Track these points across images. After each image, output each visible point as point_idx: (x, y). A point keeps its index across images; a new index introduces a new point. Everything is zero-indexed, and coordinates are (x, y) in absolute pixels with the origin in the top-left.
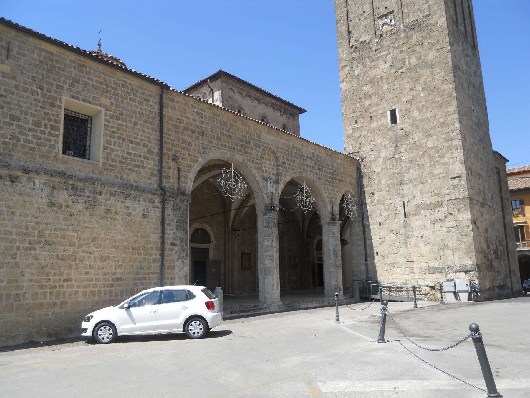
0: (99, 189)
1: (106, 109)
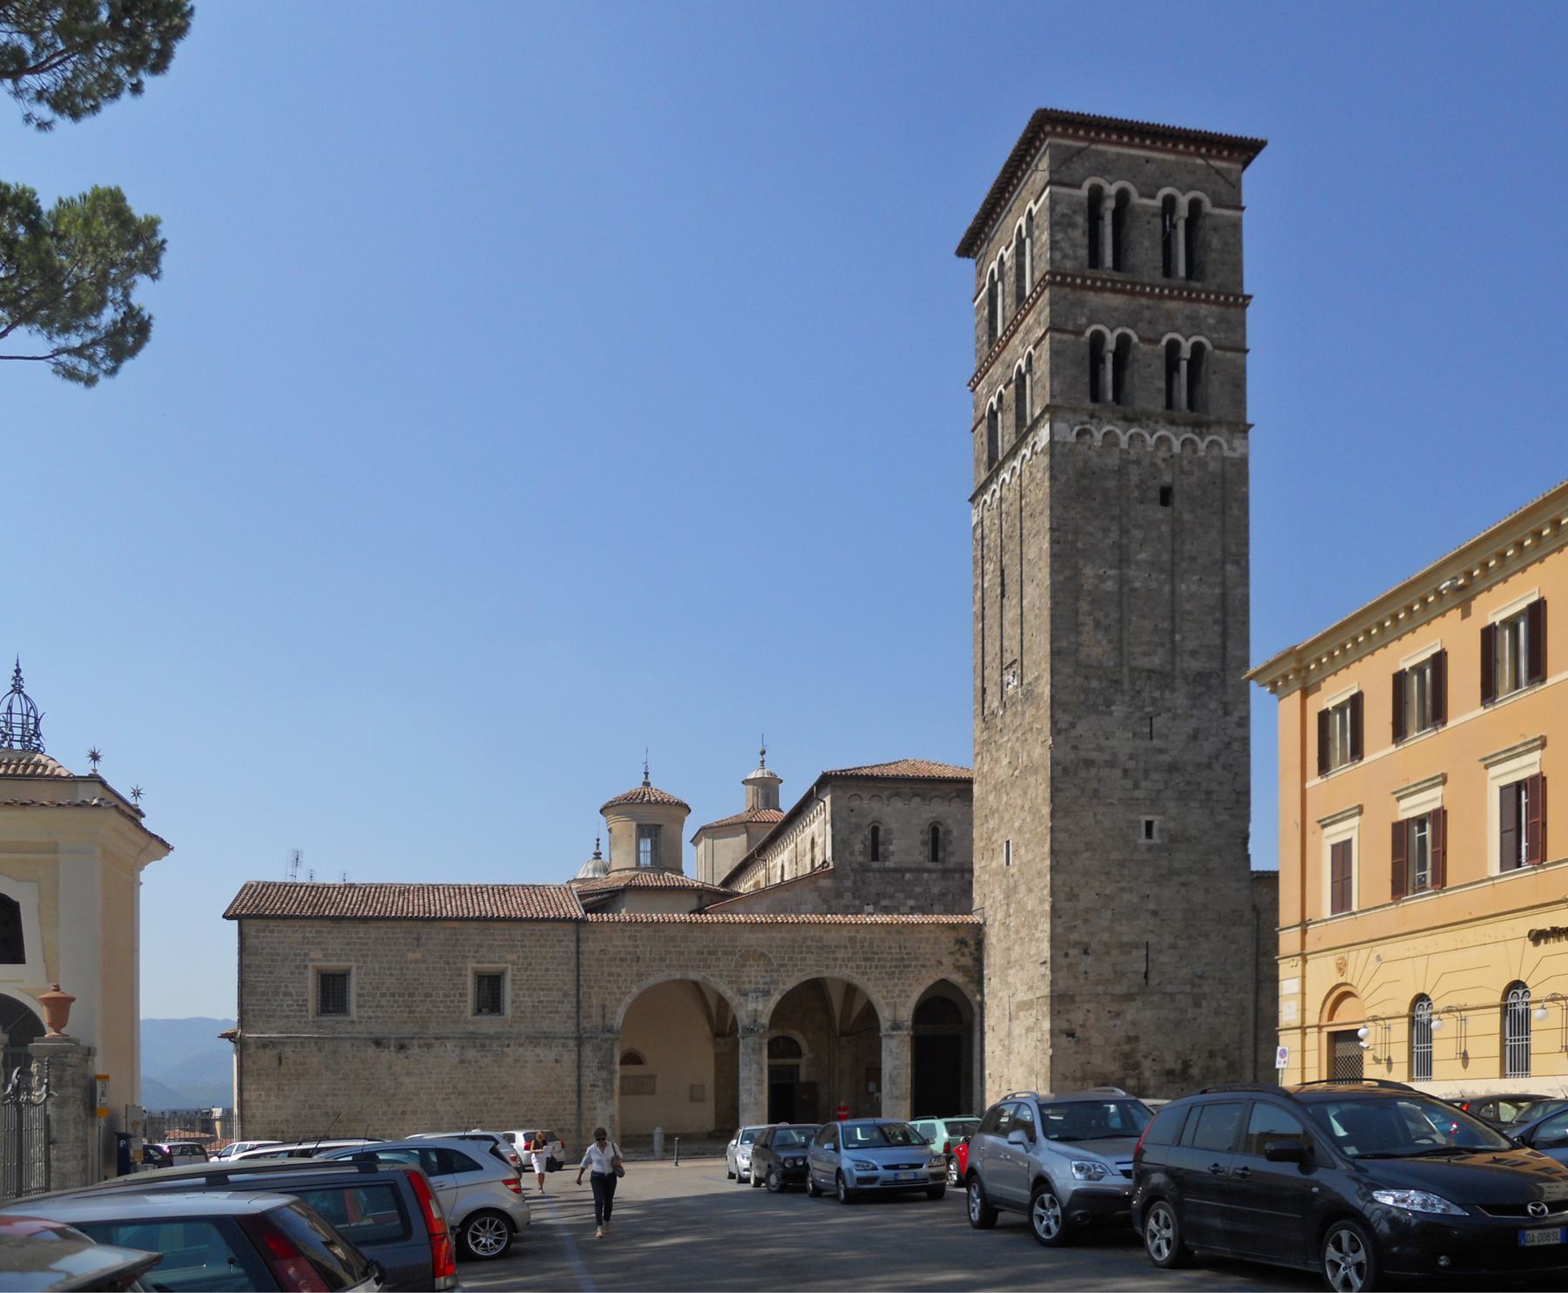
0: (506, 1042)
1: (513, 963)
